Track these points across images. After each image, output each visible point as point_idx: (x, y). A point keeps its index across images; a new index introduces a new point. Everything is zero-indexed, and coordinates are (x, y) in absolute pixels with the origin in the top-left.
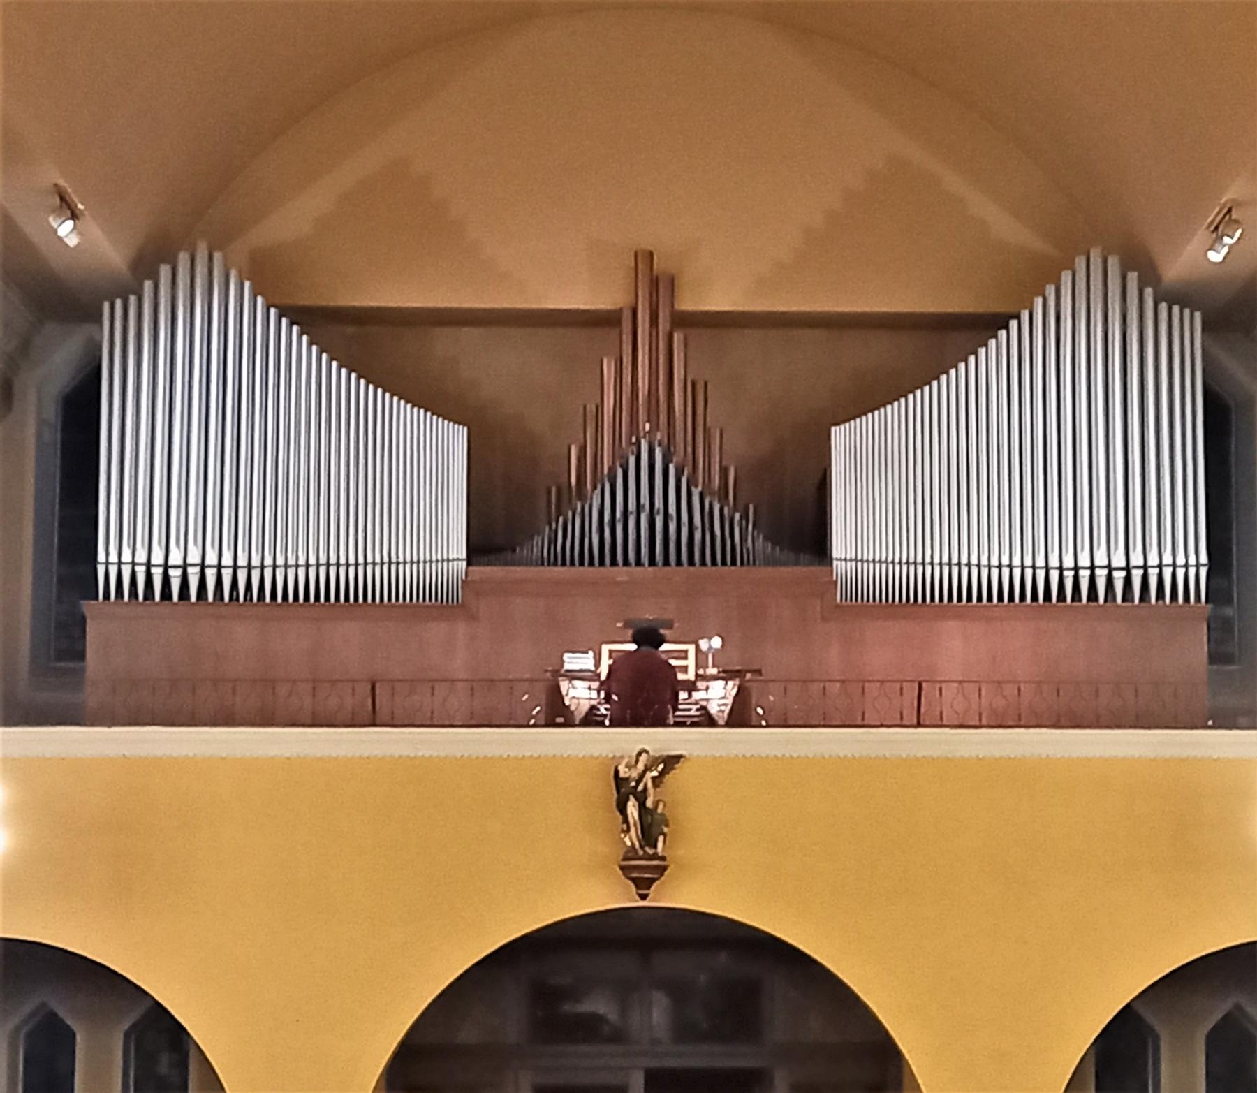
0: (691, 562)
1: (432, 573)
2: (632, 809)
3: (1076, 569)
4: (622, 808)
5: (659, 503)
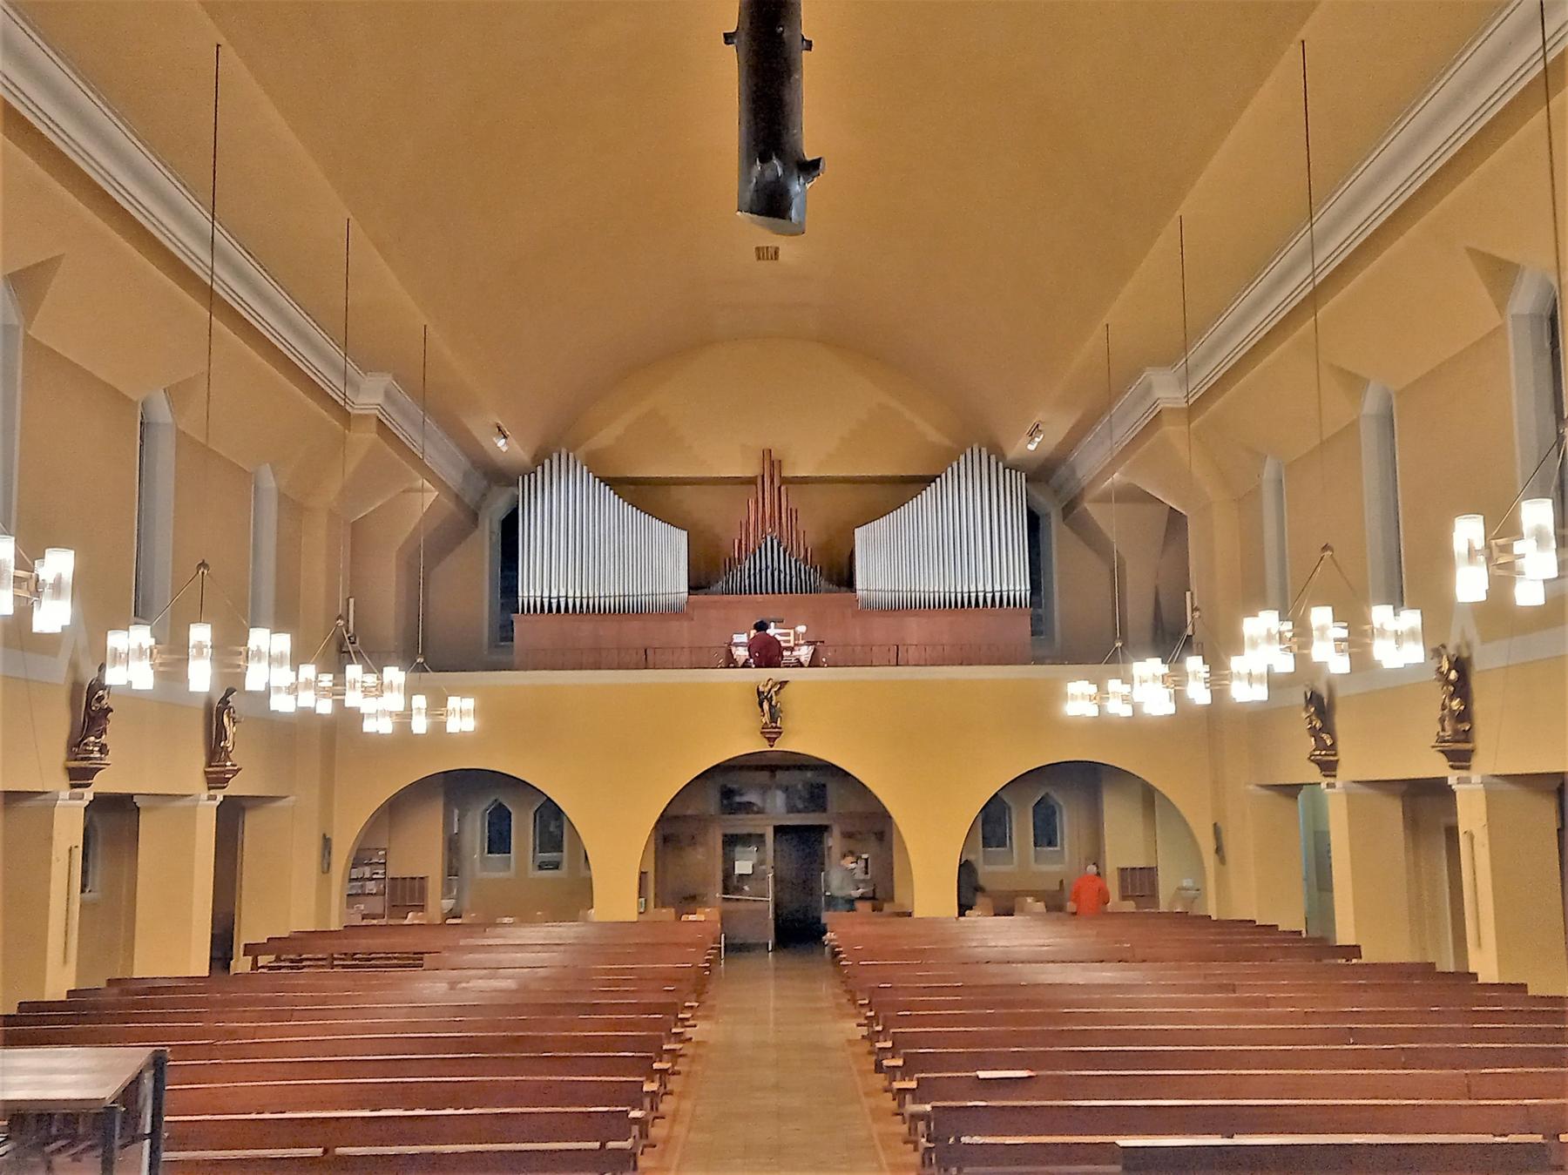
2: (766, 706)
4: (761, 705)
5: (777, 562)
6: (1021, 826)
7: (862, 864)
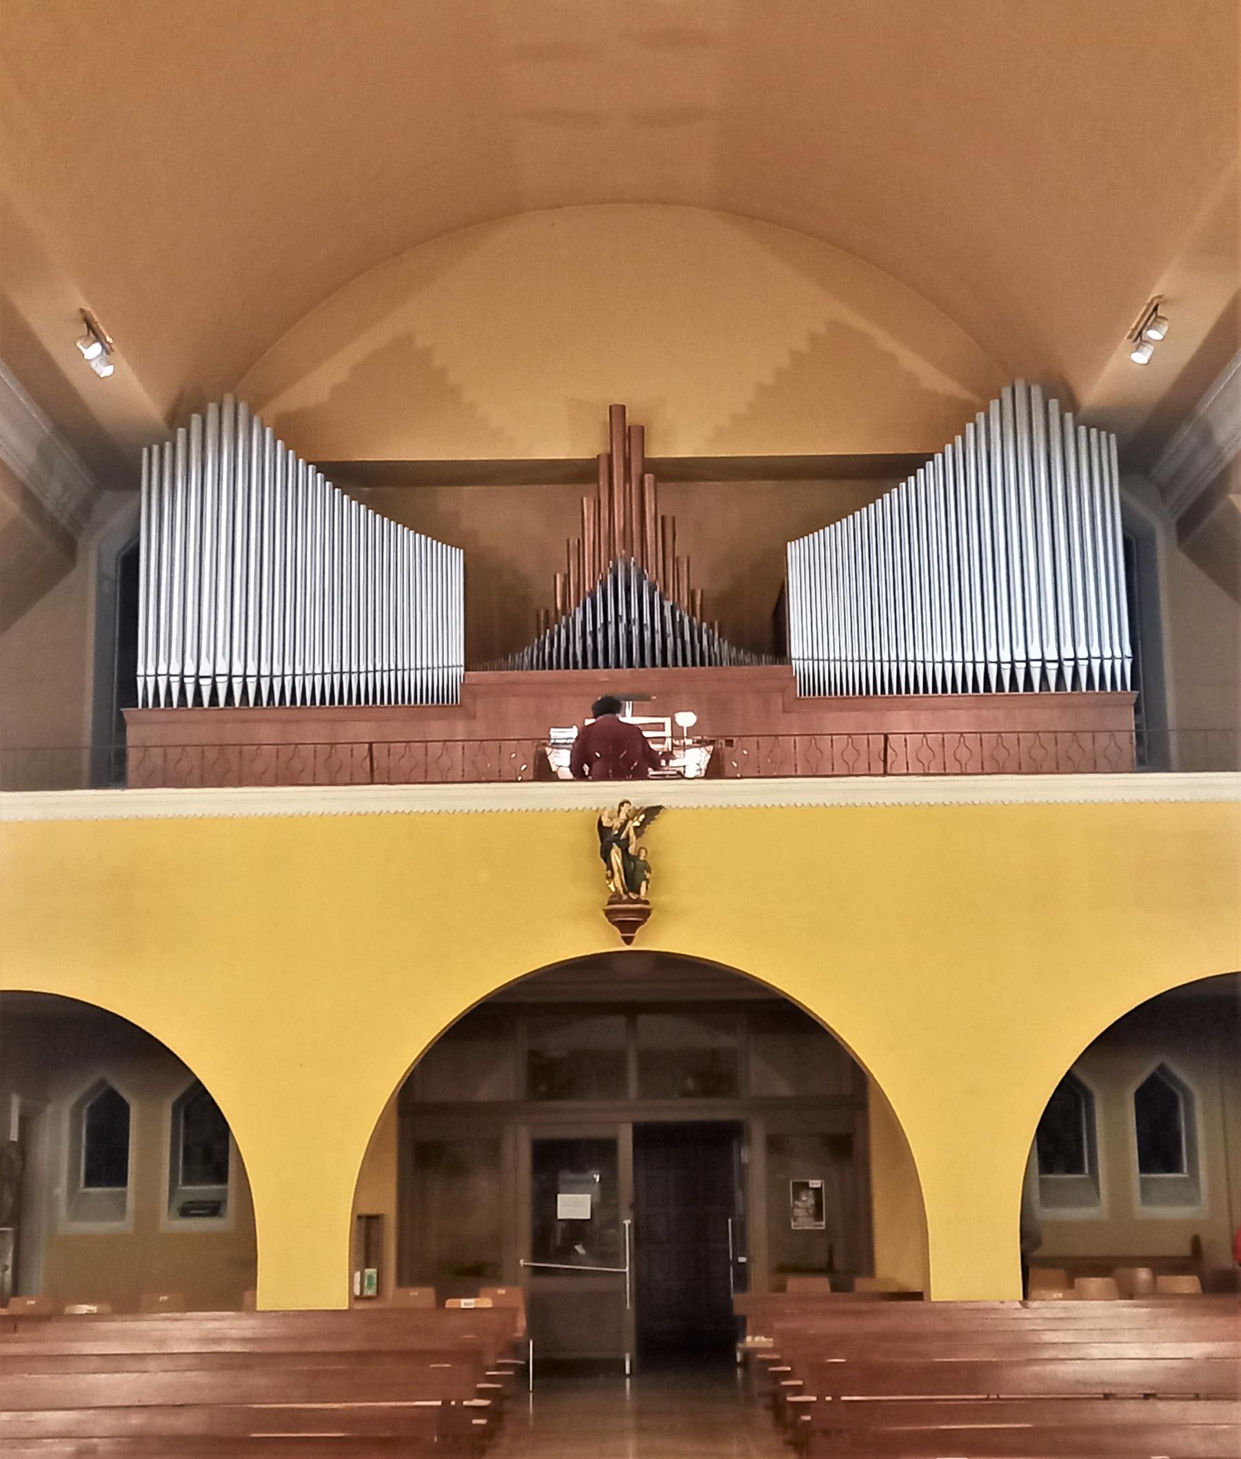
0: (665, 664)
1: (436, 679)
2: (616, 857)
3: (1013, 662)
4: (606, 855)
5: (636, 612)
6: (1115, 1131)
7: (807, 1200)
